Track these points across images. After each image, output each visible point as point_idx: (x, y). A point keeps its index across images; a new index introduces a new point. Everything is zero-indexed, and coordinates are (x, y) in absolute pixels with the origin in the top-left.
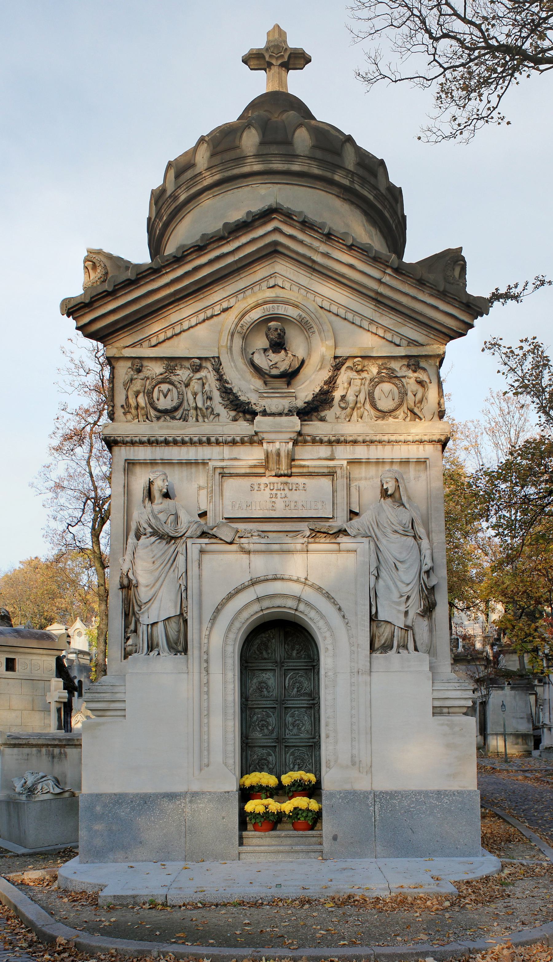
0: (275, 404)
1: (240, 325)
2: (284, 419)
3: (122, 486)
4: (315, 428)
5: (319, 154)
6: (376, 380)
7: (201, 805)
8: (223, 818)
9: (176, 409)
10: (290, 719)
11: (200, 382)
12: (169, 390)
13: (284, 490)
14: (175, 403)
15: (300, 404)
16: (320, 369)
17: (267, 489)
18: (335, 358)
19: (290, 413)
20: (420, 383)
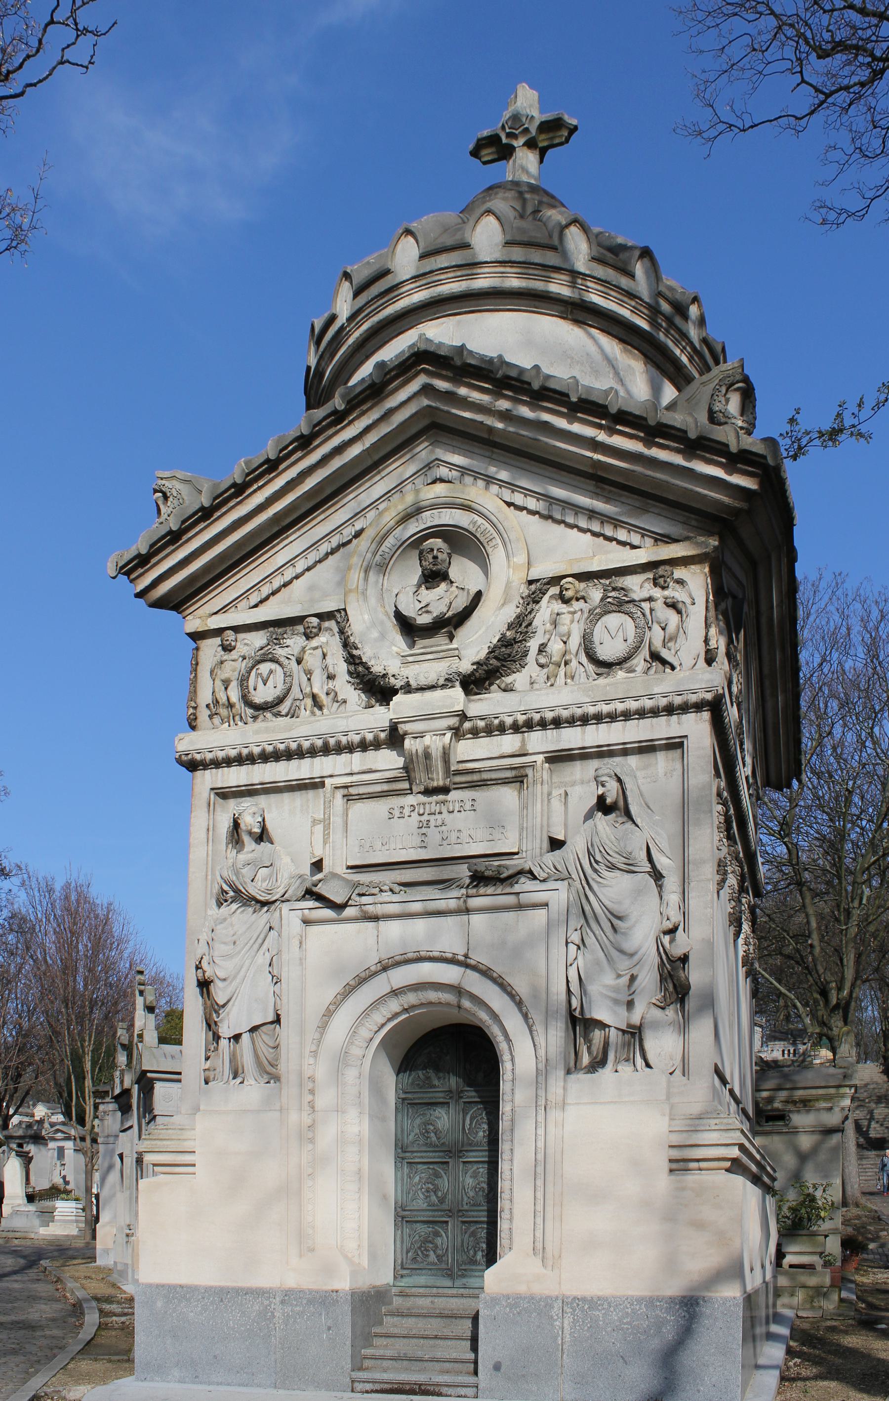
0: (433, 670)
1: (380, 553)
2: (438, 693)
3: (205, 830)
4: (490, 704)
5: (518, 254)
6: (598, 611)
7: (298, 1308)
8: (329, 1328)
9: (280, 700)
10: (471, 1180)
11: (319, 651)
12: (271, 672)
13: (440, 813)
14: (278, 692)
15: (466, 667)
16: (503, 605)
17: (415, 815)
18: (530, 582)
19: (448, 683)
20: (673, 605)
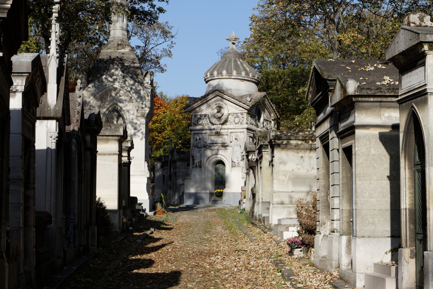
4: (224, 126)
5: (228, 75)
20: (243, 118)
